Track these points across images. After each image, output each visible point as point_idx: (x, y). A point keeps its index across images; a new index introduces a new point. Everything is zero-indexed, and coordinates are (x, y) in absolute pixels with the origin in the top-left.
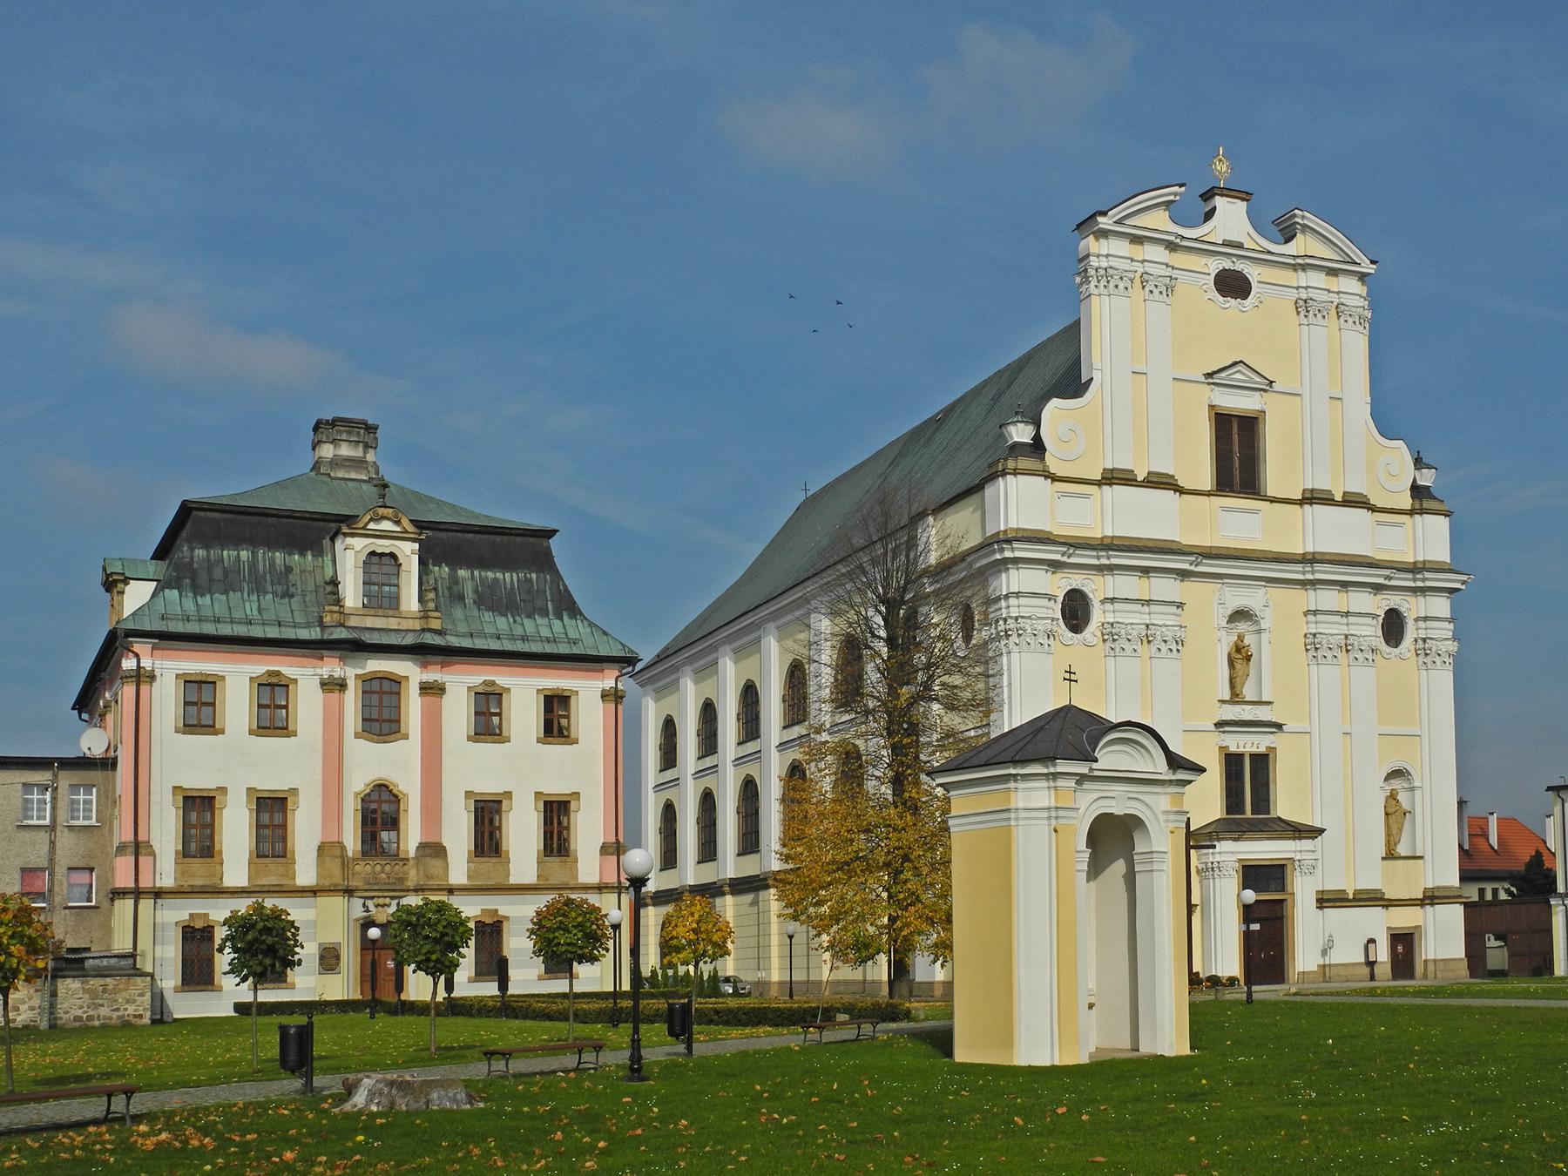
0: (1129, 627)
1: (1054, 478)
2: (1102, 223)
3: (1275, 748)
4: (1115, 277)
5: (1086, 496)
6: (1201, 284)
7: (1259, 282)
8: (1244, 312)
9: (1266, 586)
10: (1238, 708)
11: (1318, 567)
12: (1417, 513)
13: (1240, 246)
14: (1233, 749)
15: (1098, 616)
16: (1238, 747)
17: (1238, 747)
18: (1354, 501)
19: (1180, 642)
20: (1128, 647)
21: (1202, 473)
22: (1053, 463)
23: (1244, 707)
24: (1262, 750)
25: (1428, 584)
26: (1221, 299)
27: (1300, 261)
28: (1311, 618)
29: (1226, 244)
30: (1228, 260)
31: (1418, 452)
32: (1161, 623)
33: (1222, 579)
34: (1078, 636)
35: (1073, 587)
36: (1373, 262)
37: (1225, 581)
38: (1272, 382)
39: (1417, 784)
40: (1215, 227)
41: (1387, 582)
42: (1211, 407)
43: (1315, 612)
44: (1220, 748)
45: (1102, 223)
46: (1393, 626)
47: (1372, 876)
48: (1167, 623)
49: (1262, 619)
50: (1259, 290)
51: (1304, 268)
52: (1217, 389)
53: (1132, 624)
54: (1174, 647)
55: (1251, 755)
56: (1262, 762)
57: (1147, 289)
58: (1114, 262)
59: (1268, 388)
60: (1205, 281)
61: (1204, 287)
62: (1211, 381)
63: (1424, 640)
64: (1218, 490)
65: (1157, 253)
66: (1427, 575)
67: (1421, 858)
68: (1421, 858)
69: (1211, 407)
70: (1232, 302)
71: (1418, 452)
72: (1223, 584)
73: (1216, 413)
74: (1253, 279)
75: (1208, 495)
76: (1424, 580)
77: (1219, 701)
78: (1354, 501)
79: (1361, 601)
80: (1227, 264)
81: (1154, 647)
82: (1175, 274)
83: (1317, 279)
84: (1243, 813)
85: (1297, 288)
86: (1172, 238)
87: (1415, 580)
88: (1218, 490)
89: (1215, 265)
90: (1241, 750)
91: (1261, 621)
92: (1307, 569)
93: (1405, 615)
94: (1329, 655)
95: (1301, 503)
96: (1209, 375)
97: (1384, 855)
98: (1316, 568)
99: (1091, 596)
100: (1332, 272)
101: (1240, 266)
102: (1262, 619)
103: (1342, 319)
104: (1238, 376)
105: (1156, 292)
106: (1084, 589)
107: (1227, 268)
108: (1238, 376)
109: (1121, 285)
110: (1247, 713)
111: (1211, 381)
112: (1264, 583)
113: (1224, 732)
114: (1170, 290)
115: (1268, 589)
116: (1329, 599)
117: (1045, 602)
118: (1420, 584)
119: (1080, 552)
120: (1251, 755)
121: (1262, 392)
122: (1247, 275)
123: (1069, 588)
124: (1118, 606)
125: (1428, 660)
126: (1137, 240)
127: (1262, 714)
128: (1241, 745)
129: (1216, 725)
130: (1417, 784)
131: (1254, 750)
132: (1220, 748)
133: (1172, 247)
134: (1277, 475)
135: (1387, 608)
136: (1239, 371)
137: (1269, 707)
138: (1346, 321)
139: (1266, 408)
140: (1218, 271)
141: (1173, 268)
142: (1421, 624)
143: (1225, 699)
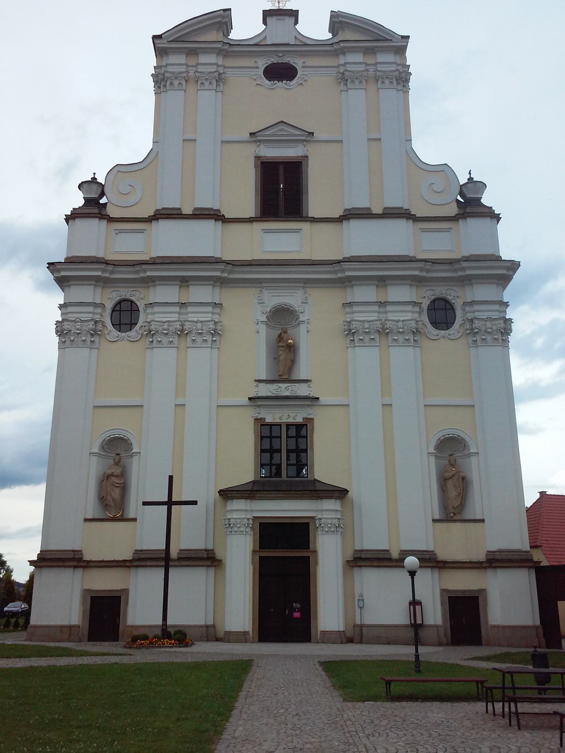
0: (166, 324)
1: (111, 220)
2: (159, 44)
3: (312, 419)
4: (172, 78)
5: (141, 231)
7: (303, 67)
8: (289, 89)
9: (303, 288)
10: (275, 386)
11: (345, 265)
12: (461, 218)
13: (288, 45)
14: (269, 419)
15: (142, 318)
19: (215, 333)
20: (165, 340)
22: (112, 211)
23: (280, 385)
24: (299, 420)
25: (469, 272)
27: (336, 46)
28: (348, 310)
30: (276, 57)
32: (196, 319)
33: (261, 283)
35: (123, 297)
37: (263, 285)
38: (313, 133)
39: (473, 450)
40: (266, 36)
41: (424, 274)
42: (257, 158)
43: (350, 304)
44: (256, 419)
45: (159, 44)
48: (201, 319)
49: (302, 313)
50: (303, 73)
51: (343, 52)
52: (262, 146)
53: (169, 321)
54: (209, 338)
57: (199, 83)
58: (170, 69)
59: (308, 139)
60: (255, 73)
62: (254, 139)
63: (471, 321)
64: (261, 217)
65: (212, 59)
66: (465, 264)
67: (483, 521)
68: (483, 521)
69: (257, 158)
72: (262, 287)
73: (261, 162)
76: (464, 269)
77: (255, 380)
80: (275, 60)
81: (189, 339)
82: (229, 72)
83: (358, 58)
84: (281, 477)
85: (338, 67)
86: (220, 46)
87: (456, 271)
88: (261, 217)
89: (263, 63)
90: (277, 421)
91: (301, 315)
92: (336, 268)
93: (453, 301)
94: (367, 338)
95: (341, 219)
97: (437, 517)
98: (344, 267)
99: (138, 303)
100: (370, 51)
101: (286, 60)
102: (302, 313)
103: (380, 82)
106: (133, 299)
107: (275, 62)
109: (176, 83)
110: (284, 389)
111: (254, 139)
112: (302, 285)
113: (259, 406)
114: (220, 79)
115: (307, 290)
117: (91, 309)
118: (460, 274)
119: (119, 269)
121: (305, 143)
122: (293, 64)
123: (118, 298)
124: (156, 309)
125: (478, 338)
126: (192, 52)
127: (302, 390)
129: (250, 399)
130: (473, 450)
131: (291, 420)
132: (256, 419)
135: (433, 298)
136: (282, 130)
137: (307, 384)
138: (383, 82)
139: (309, 154)
140: (267, 65)
141: (225, 67)
142: (468, 309)
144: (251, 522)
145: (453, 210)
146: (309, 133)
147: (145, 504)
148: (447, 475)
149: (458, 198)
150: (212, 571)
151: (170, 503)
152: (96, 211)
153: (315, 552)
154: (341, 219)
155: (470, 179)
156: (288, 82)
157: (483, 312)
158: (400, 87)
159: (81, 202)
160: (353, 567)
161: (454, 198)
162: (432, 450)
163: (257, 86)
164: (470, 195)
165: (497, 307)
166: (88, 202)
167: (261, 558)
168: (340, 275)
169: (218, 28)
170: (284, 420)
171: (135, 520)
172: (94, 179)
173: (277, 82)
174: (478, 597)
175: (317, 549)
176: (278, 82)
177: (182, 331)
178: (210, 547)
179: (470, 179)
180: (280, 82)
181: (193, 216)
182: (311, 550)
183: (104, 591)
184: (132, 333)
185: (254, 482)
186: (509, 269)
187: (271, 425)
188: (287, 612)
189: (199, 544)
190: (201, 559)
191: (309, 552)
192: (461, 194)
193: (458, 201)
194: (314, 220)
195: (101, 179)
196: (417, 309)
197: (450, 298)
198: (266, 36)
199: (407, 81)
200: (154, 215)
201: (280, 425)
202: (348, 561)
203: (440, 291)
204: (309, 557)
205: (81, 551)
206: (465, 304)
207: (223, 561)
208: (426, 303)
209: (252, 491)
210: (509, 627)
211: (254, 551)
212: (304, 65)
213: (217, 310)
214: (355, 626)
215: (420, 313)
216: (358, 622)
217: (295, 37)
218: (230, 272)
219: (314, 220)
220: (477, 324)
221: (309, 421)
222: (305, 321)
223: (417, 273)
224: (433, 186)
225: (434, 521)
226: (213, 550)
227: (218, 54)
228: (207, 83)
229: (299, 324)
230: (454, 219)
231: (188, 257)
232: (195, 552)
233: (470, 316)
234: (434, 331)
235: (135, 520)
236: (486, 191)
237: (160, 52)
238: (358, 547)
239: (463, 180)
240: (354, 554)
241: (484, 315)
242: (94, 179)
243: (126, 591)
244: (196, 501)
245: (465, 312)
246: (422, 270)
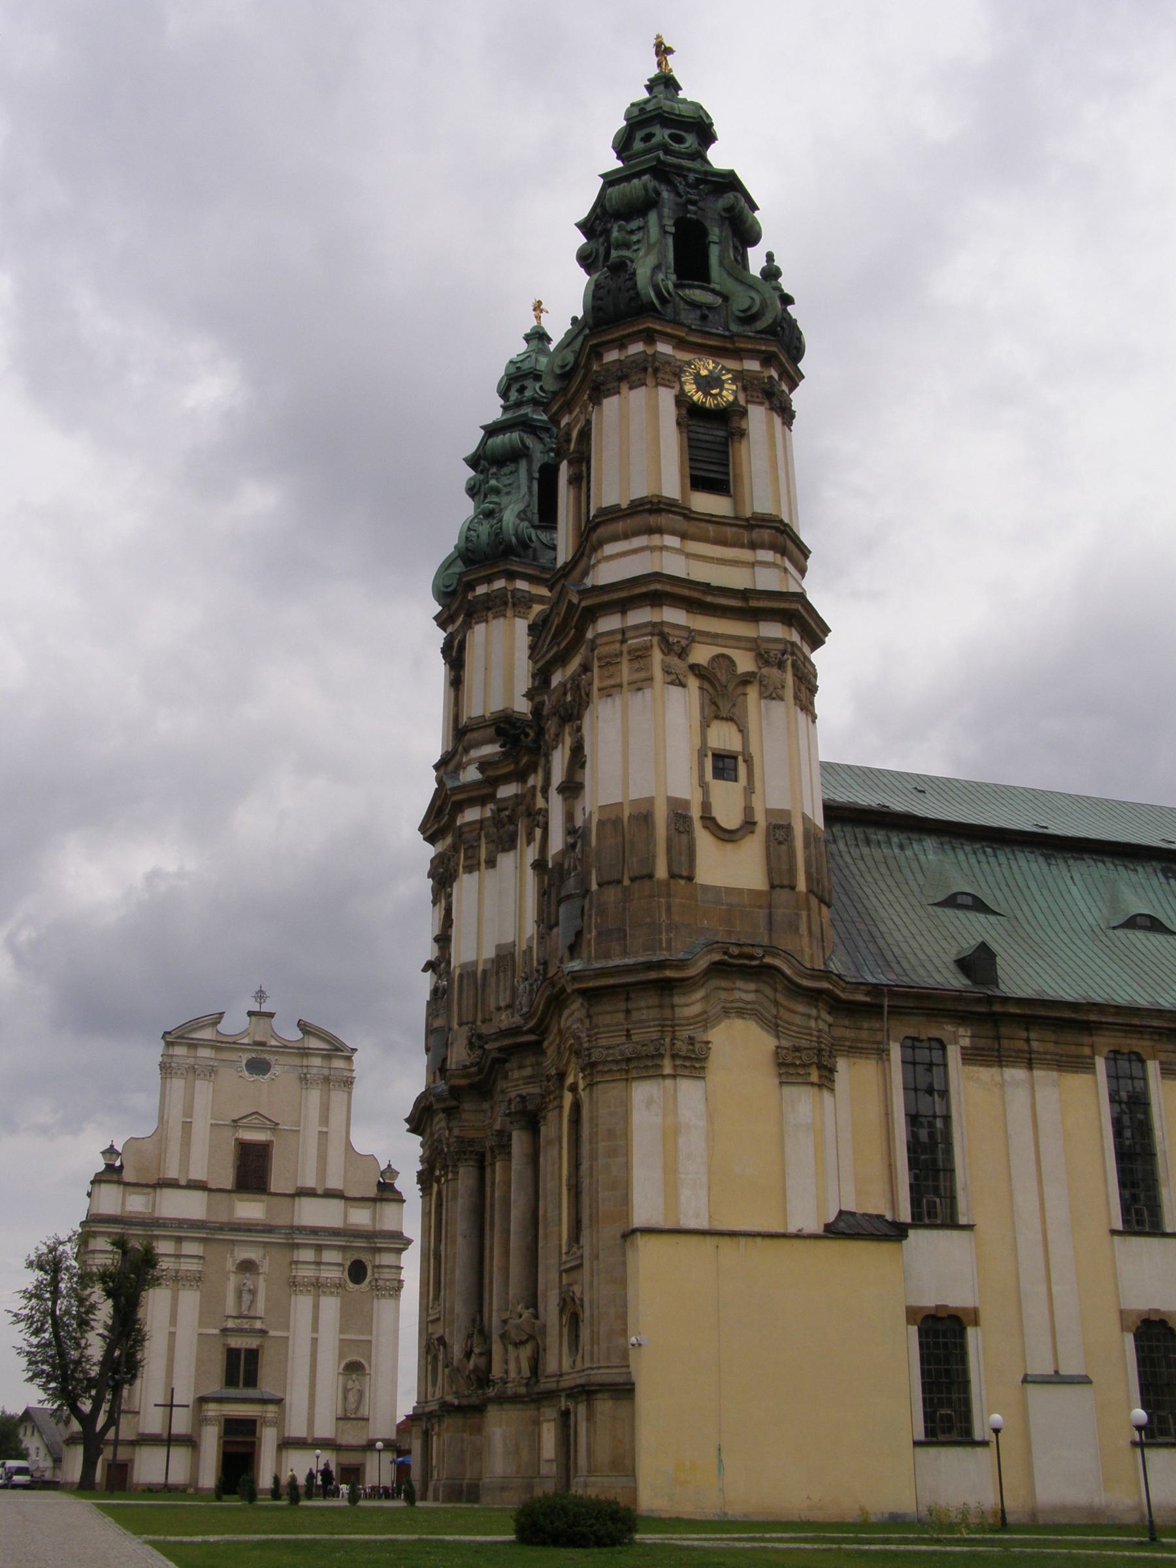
18: (330, 1194)
21: (227, 1179)
24: (254, 1346)
25: (378, 1245)
38: (278, 1124)
46: (357, 1272)
47: (325, 1429)
56: (253, 1355)
63: (377, 1280)
74: (273, 1063)
78: (330, 1194)
79: (330, 1256)
89: (245, 1057)
90: (238, 1346)
95: (293, 1196)
96: (234, 1121)
100: (328, 1057)
104: (256, 1121)
105: (202, 1075)
108: (256, 1121)
126: (193, 1045)
127: (258, 1325)
128: (239, 1343)
131: (248, 1346)
133: (213, 1047)
134: (277, 1183)
142: (376, 1270)
145: (372, 1192)
147: (156, 1405)
148: (349, 1387)
151: (171, 1406)
152: (115, 1177)
153: (260, 1439)
154: (293, 1196)
155: (389, 1166)
157: (387, 1274)
158: (346, 1089)
159: (102, 1167)
162: (341, 1371)
165: (394, 1270)
166: (110, 1167)
167: (224, 1442)
168: (290, 1241)
172: (112, 1146)
177: (176, 1277)
179: (389, 1166)
186: (405, 1244)
193: (379, 1182)
195: (119, 1148)
196: (341, 1269)
197: (364, 1260)
199: (352, 1083)
203: (357, 1256)
206: (374, 1267)
208: (348, 1263)
211: (220, 1438)
213: (202, 1261)
215: (343, 1271)
218: (213, 1234)
220: (380, 1283)
223: (344, 1243)
225: (338, 1419)
228: (202, 1075)
229: (259, 1274)
230: (373, 1200)
233: (376, 1276)
234: (351, 1285)
237: (169, 1044)
238: (287, 1435)
239: (383, 1167)
241: (386, 1276)
242: (112, 1146)
243: (132, 1461)
245: (373, 1273)
246: (347, 1241)
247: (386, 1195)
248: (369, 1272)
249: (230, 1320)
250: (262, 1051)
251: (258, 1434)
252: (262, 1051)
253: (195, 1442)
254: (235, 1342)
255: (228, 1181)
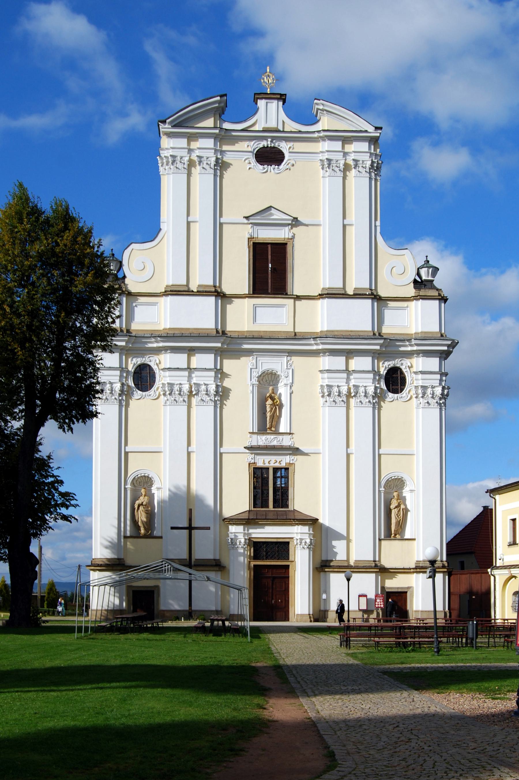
5: (155, 304)
6: (244, 159)
7: (290, 152)
14: (260, 464)
16: (264, 463)
17: (264, 463)
24: (283, 465)
26: (261, 167)
29: (265, 131)
31: (427, 257)
34: (144, 393)
36: (377, 128)
40: (257, 120)
48: (206, 383)
55: (274, 468)
61: (247, 161)
64: (254, 293)
67: (414, 539)
70: (271, 168)
71: (427, 257)
75: (245, 297)
77: (250, 433)
83: (337, 145)
84: (267, 507)
90: (267, 465)
96: (247, 218)
116: (339, 362)
120: (274, 468)
128: (267, 462)
129: (245, 448)
131: (277, 465)
133: (216, 137)
143: (254, 431)
144: (247, 541)
146: (294, 218)
149: (416, 278)
150: (219, 573)
156: (277, 167)
160: (320, 572)
161: (413, 279)
163: (250, 169)
164: (424, 278)
169: (215, 112)
170: (273, 465)
171: (161, 537)
173: (267, 166)
174: (406, 592)
175: (296, 560)
176: (268, 165)
177: (191, 392)
178: (218, 558)
180: (269, 166)
181: (197, 293)
182: (290, 560)
183: (143, 587)
184: (151, 392)
185: (249, 511)
187: (261, 469)
188: (273, 602)
189: (210, 556)
190: (212, 566)
191: (289, 561)
192: (418, 274)
194: (298, 298)
198: (257, 120)
200: (165, 292)
201: (268, 468)
202: (317, 568)
204: (289, 566)
205: (123, 559)
207: (227, 566)
209: (248, 519)
210: (426, 611)
212: (291, 150)
214: (320, 611)
216: (322, 608)
217: (283, 121)
219: (298, 298)
221: (290, 465)
222: (288, 384)
224: (395, 268)
226: (219, 560)
227: (215, 138)
231: (194, 329)
232: (206, 561)
235: (161, 537)
236: (438, 272)
240: (321, 563)
244: (210, 527)
247: (422, 292)
248: (408, 380)
249: (255, 436)
250: (273, 138)
251: (291, 558)
252: (273, 138)
253: (225, 567)
254: (262, 461)
255: (244, 287)
